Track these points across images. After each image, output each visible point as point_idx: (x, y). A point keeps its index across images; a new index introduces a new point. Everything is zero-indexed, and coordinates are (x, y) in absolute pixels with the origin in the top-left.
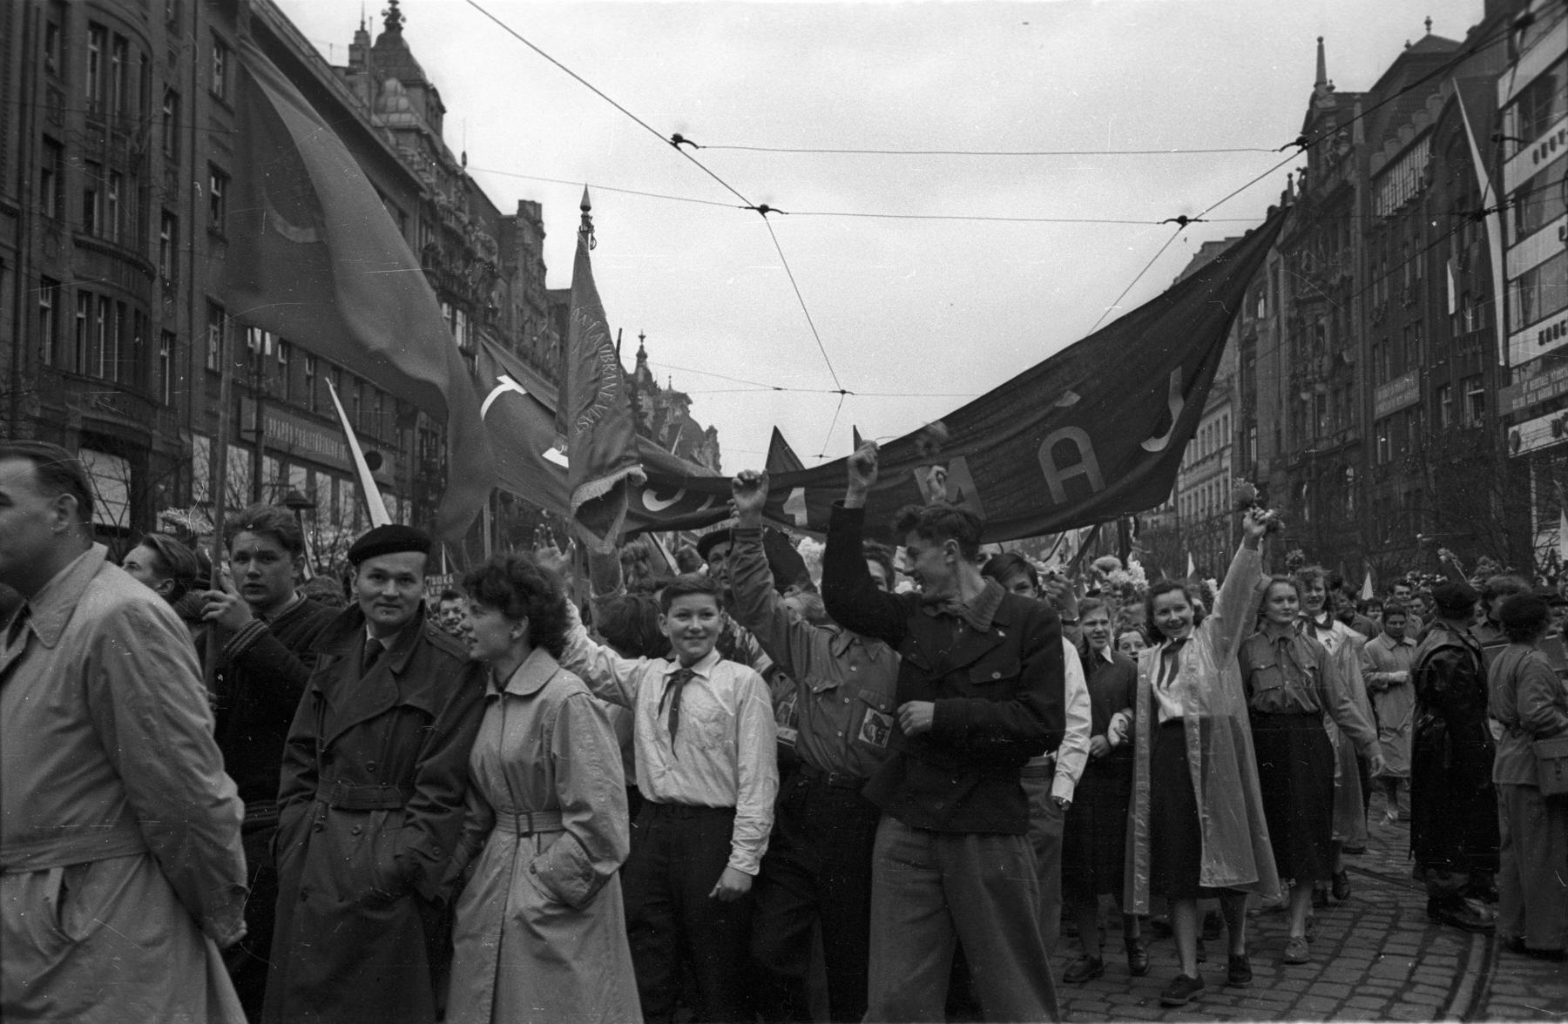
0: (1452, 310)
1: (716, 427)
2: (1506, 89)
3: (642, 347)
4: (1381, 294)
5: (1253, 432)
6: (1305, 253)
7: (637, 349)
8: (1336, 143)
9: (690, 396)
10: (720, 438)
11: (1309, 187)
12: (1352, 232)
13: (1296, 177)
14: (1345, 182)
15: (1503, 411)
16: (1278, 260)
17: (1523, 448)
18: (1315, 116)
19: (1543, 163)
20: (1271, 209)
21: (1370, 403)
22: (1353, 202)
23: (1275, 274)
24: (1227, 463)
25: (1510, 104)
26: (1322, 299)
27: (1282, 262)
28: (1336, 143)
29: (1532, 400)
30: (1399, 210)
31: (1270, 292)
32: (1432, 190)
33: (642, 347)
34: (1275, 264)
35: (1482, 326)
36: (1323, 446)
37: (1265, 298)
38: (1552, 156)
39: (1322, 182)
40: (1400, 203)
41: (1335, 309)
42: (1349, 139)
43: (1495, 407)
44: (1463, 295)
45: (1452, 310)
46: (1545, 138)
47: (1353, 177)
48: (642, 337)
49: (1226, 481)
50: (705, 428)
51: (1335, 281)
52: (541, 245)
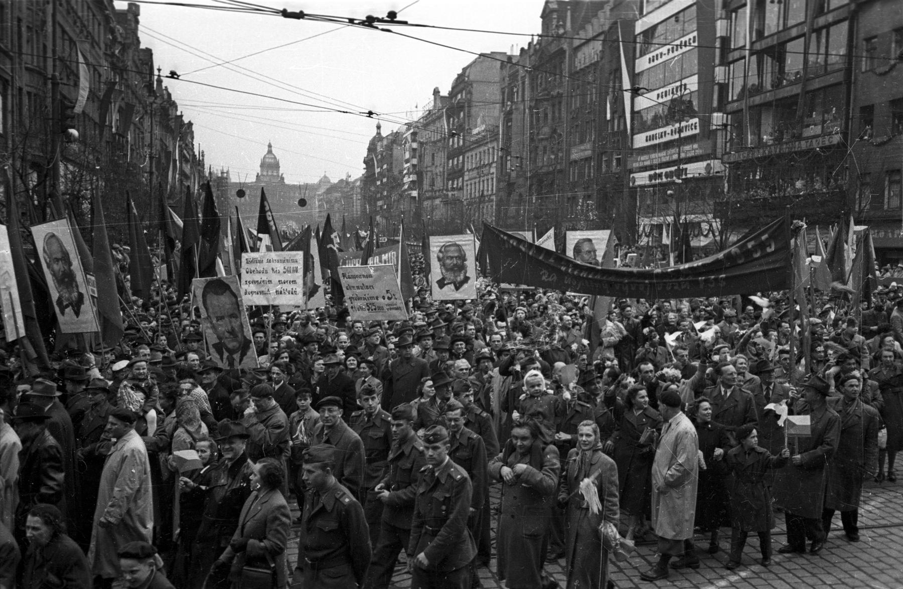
0: (609, 116)
2: (640, 26)
4: (576, 103)
5: (509, 158)
8: (558, 27)
10: (194, 128)
11: (543, 44)
13: (536, 39)
14: (562, 48)
15: (629, 167)
17: (637, 183)
18: (547, 11)
19: (652, 64)
20: (522, 49)
21: (568, 153)
22: (565, 58)
24: (493, 170)
25: (639, 34)
26: (547, 100)
28: (558, 27)
29: (641, 164)
30: (588, 67)
31: (520, 90)
32: (603, 61)
35: (622, 127)
36: (544, 170)
37: (517, 92)
38: (656, 62)
39: (550, 44)
40: (588, 64)
41: (553, 106)
42: (564, 26)
43: (625, 165)
44: (613, 113)
45: (609, 116)
46: (654, 54)
47: (565, 47)
49: (492, 179)
51: (554, 93)
52: (136, 29)
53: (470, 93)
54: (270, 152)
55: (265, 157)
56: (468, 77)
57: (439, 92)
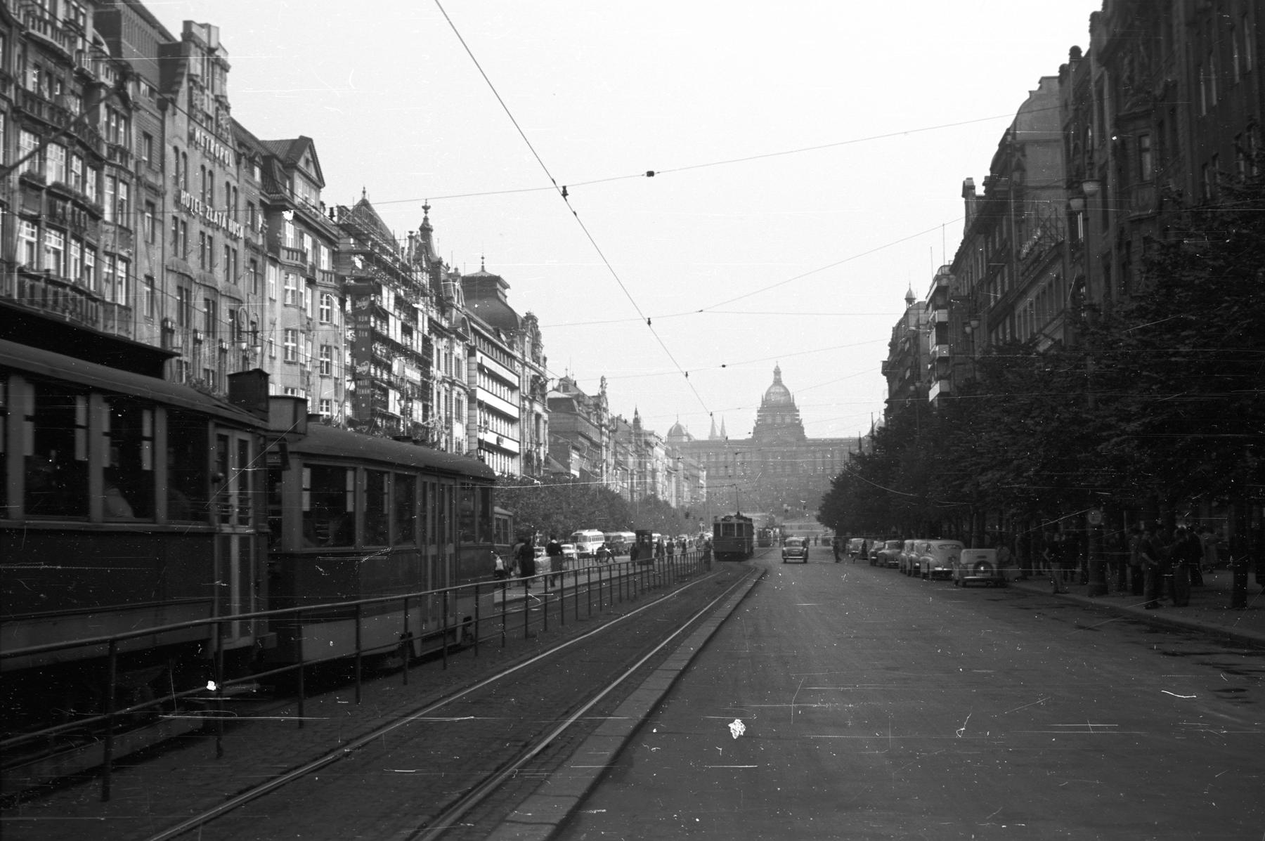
1: (536, 314)
3: (426, 219)
6: (1126, 61)
7: (421, 222)
9: (505, 278)
12: (1175, 22)
16: (1101, 77)
20: (1094, 16)
23: (1100, 93)
26: (1147, 114)
27: (1106, 78)
33: (426, 219)
34: (1100, 81)
41: (1161, 125)
48: (426, 208)
50: (521, 313)
51: (1158, 92)
53: (1021, 168)
54: (778, 382)
55: (768, 393)
56: (1014, 135)
57: (973, 187)
